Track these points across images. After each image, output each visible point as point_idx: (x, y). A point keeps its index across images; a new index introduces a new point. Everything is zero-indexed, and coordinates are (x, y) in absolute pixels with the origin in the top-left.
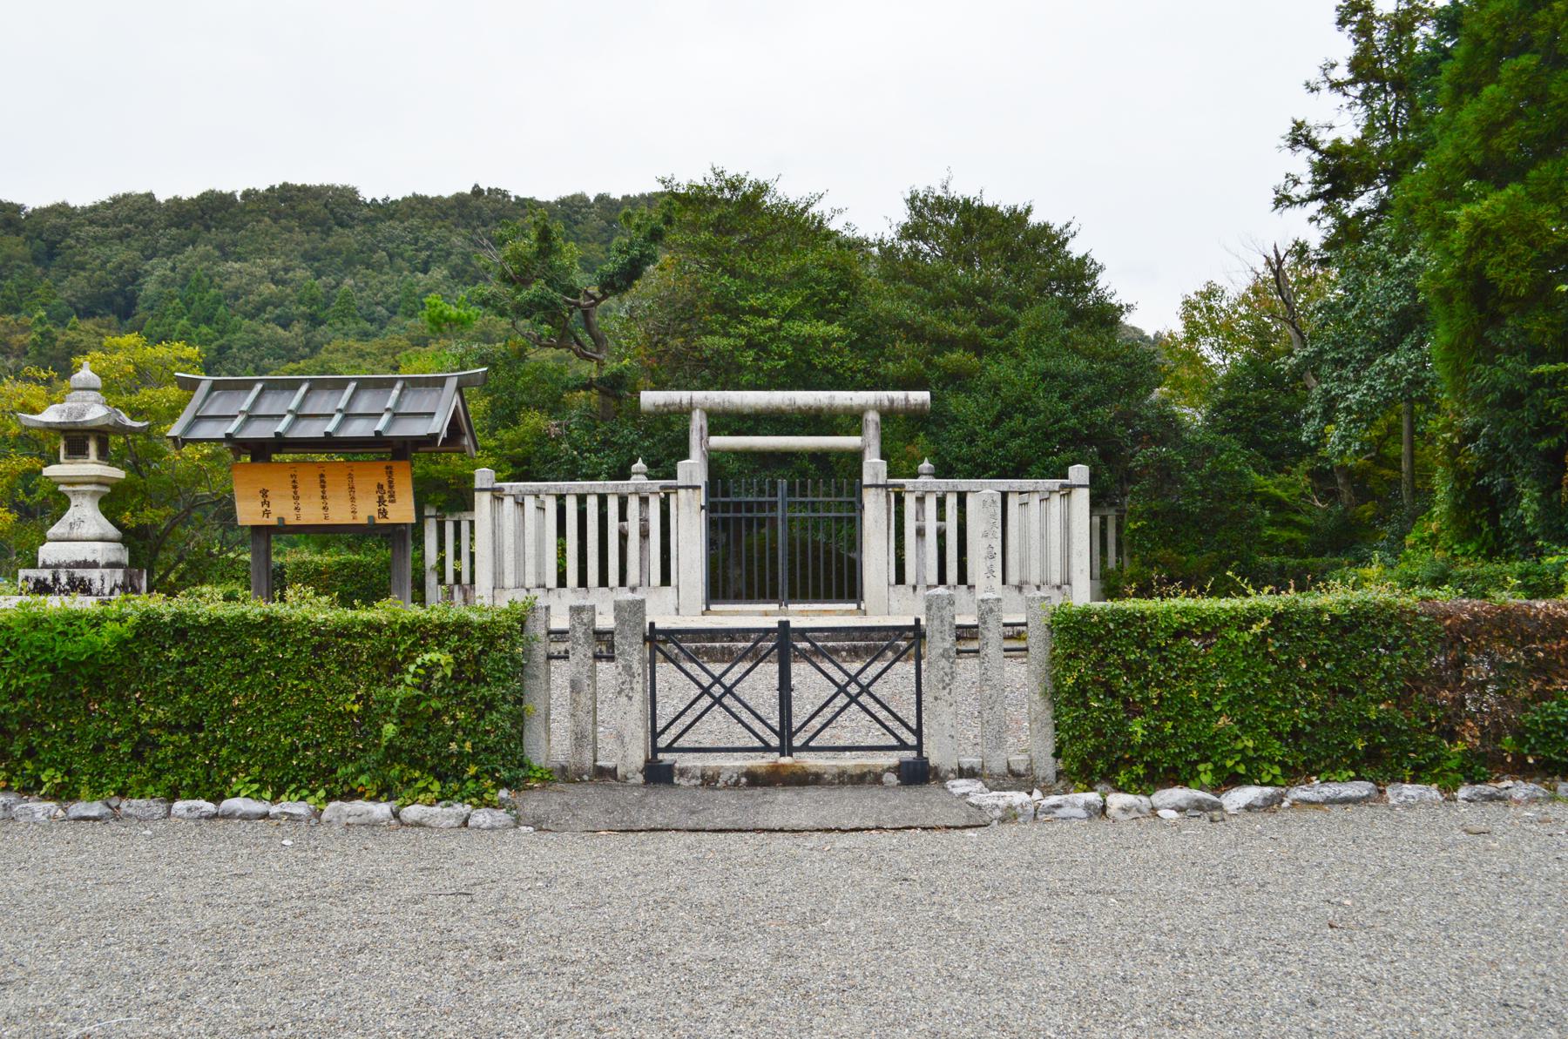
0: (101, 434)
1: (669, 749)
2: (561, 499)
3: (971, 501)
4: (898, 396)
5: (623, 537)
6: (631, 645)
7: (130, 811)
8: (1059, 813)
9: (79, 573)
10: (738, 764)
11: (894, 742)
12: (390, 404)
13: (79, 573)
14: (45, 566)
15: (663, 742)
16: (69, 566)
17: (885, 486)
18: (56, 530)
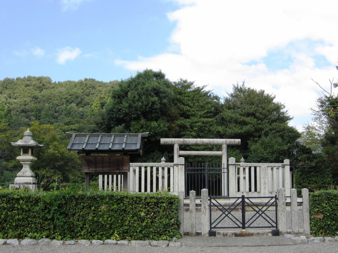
0: (32, 148)
1: (214, 227)
2: (140, 168)
3: (258, 169)
4: (232, 140)
5: (157, 178)
6: (205, 201)
7: (81, 243)
8: (314, 241)
9: (26, 185)
10: (232, 231)
11: (271, 225)
12: (125, 141)
13: (26, 185)
14: (17, 184)
15: (213, 226)
16: (23, 184)
17: (235, 165)
18: (19, 174)
